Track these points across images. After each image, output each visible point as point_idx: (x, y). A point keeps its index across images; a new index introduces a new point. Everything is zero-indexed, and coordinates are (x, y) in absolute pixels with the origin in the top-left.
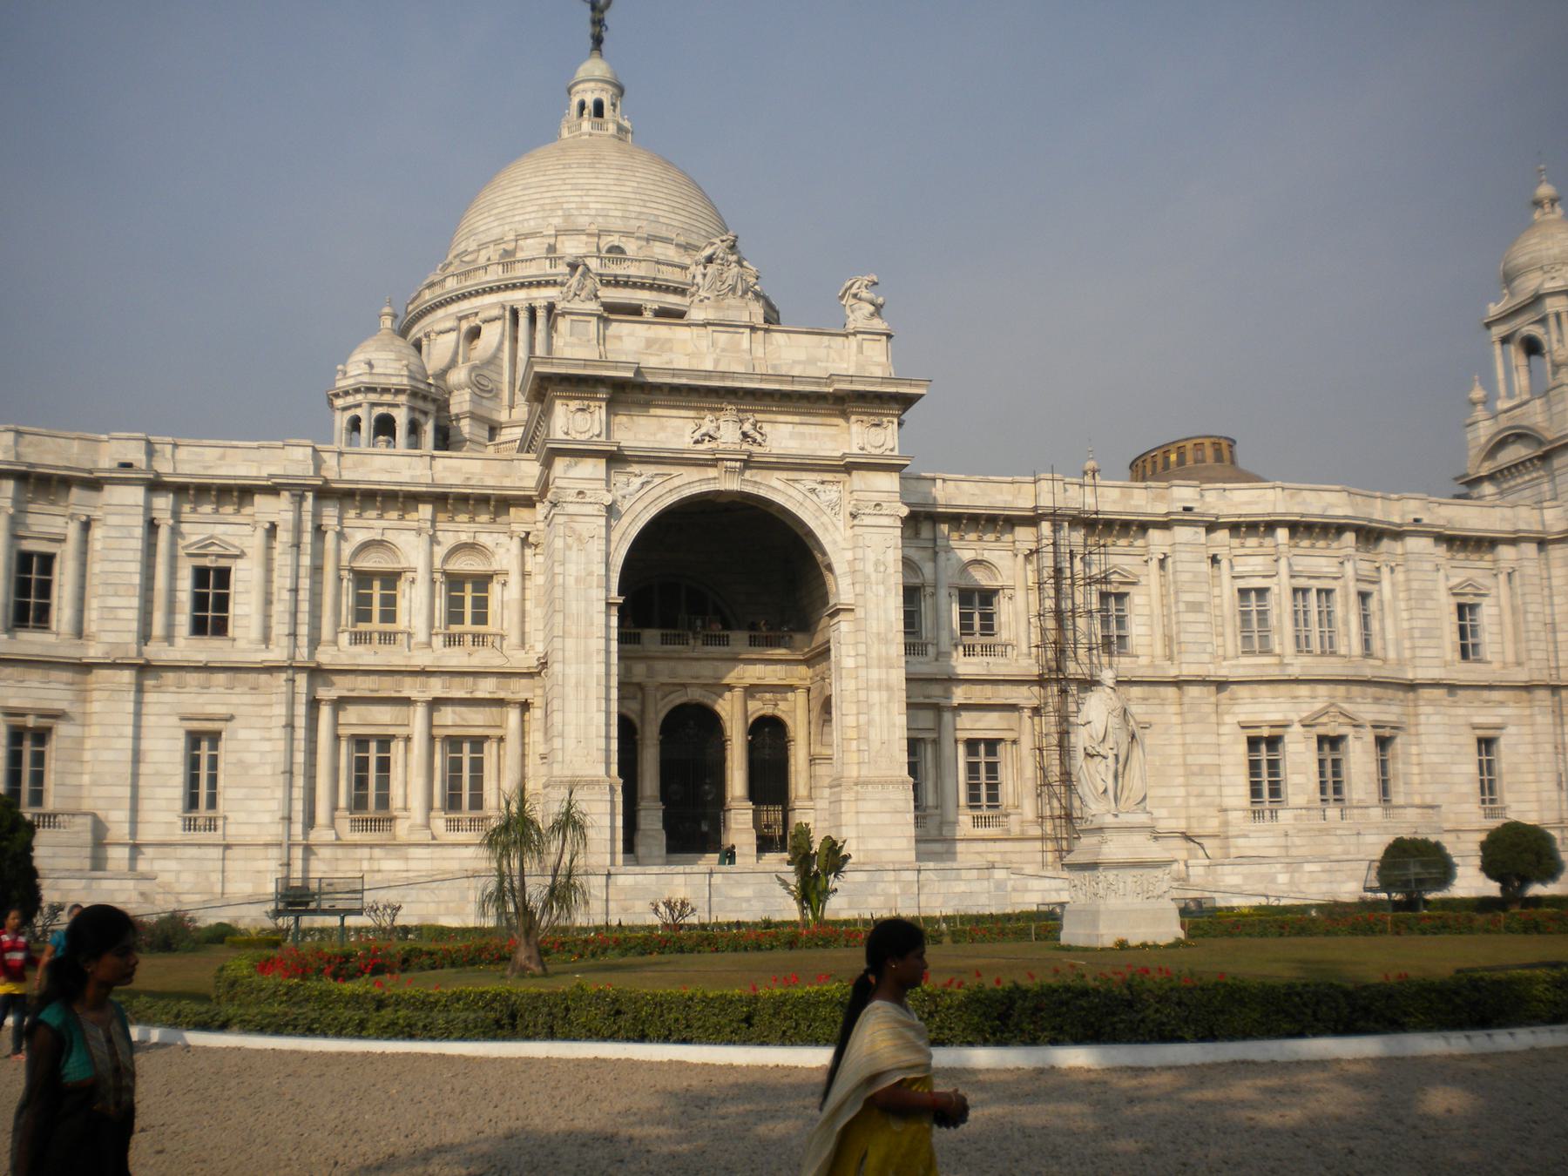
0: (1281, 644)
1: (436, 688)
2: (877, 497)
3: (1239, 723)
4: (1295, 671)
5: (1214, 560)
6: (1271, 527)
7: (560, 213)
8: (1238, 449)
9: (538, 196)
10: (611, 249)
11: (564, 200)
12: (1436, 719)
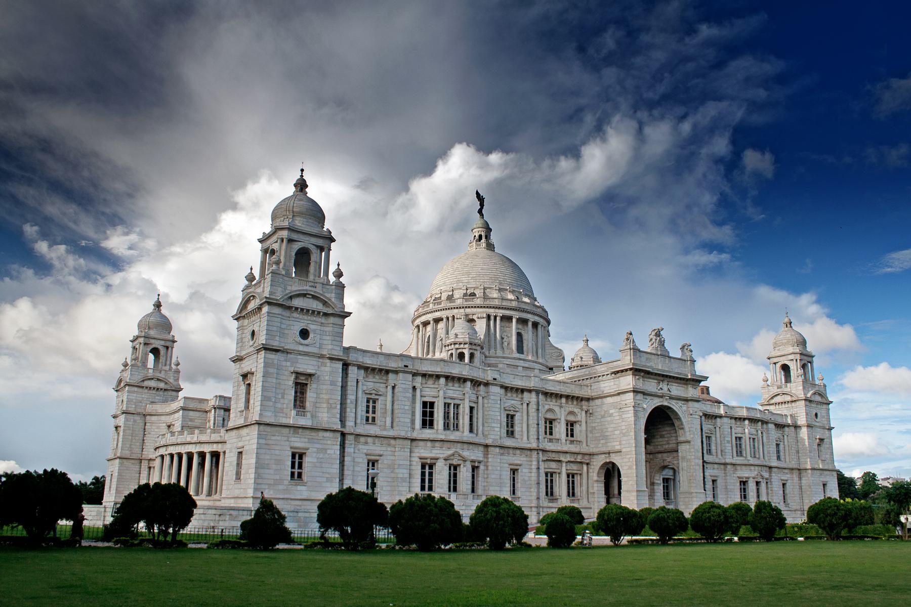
0: (746, 454)
1: (568, 458)
2: (696, 410)
3: (738, 477)
5: (731, 428)
6: (745, 419)
8: (710, 389)
9: (488, 273)
11: (498, 277)
12: (776, 477)
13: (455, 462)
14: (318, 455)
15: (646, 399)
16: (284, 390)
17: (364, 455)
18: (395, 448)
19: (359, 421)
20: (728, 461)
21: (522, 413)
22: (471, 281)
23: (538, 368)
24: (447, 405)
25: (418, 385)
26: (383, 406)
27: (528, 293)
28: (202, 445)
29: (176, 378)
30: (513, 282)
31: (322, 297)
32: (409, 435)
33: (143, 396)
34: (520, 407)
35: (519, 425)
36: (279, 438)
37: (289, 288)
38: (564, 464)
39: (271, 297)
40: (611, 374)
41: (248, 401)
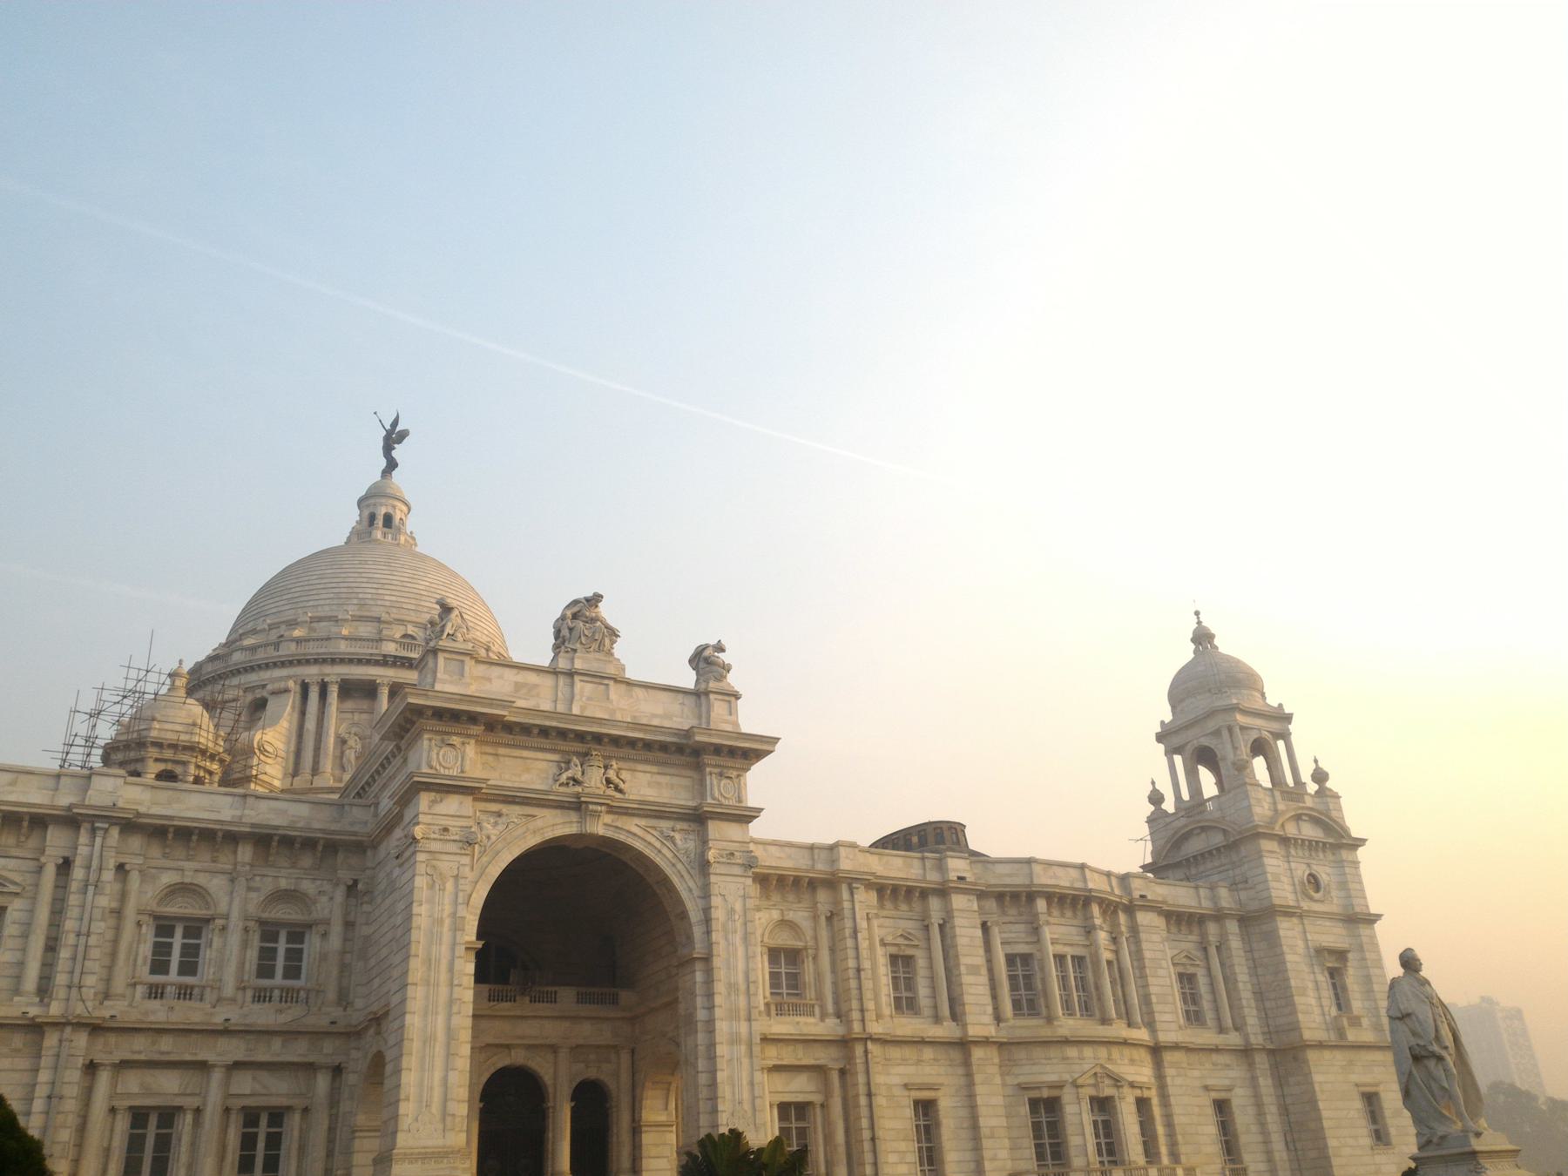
7: (355, 601)
9: (334, 585)
10: (405, 636)
12: (1179, 1081)
15: (499, 815)
20: (974, 1031)
38: (217, 1076)
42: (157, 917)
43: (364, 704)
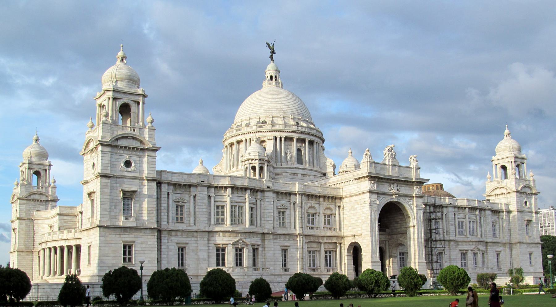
0: (466, 233)
1: (325, 240)
4: (470, 239)
7: (283, 112)
9: (276, 106)
12: (491, 249)
13: (240, 246)
14: (142, 245)
15: (380, 197)
16: (116, 203)
17: (175, 244)
18: (197, 238)
19: (170, 221)
20: (451, 238)
21: (290, 209)
22: (262, 112)
23: (314, 174)
24: (233, 207)
25: (212, 194)
26: (188, 210)
27: (306, 119)
28: (70, 241)
29: (54, 192)
30: (294, 111)
31: (139, 138)
32: (207, 229)
33: (31, 206)
34: (288, 205)
35: (289, 218)
36: (114, 236)
37: (115, 132)
38: (322, 245)
39: (103, 140)
40: (355, 180)
41: (92, 212)
42: (308, 213)
43: (290, 143)
